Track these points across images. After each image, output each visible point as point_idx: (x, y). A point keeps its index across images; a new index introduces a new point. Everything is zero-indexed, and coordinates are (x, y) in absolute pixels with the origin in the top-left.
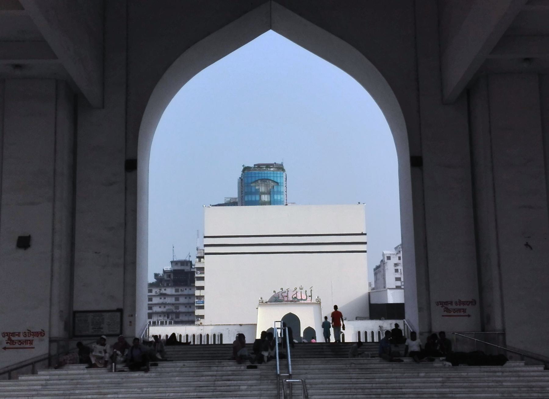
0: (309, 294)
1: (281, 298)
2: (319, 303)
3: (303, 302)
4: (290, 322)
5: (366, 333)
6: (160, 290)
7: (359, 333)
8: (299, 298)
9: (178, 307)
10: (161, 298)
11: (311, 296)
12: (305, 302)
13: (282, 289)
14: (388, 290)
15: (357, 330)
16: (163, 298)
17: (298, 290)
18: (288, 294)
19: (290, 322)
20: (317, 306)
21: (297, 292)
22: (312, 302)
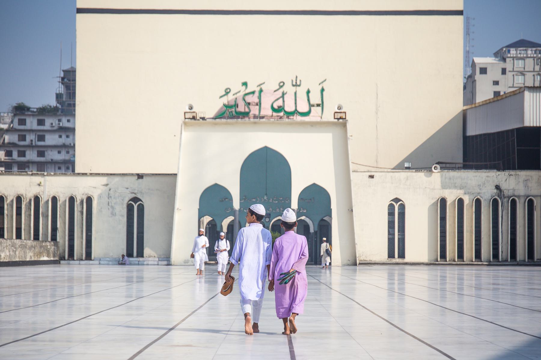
0: (315, 99)
1: (242, 108)
2: (341, 120)
3: (299, 118)
6: (60, 121)
8: (289, 107)
9: (25, 136)
10: (60, 137)
11: (321, 105)
12: (306, 119)
13: (245, 84)
14: (527, 94)
16: (64, 136)
18: (260, 97)
20: (338, 130)
21: (284, 94)
22: (324, 119)
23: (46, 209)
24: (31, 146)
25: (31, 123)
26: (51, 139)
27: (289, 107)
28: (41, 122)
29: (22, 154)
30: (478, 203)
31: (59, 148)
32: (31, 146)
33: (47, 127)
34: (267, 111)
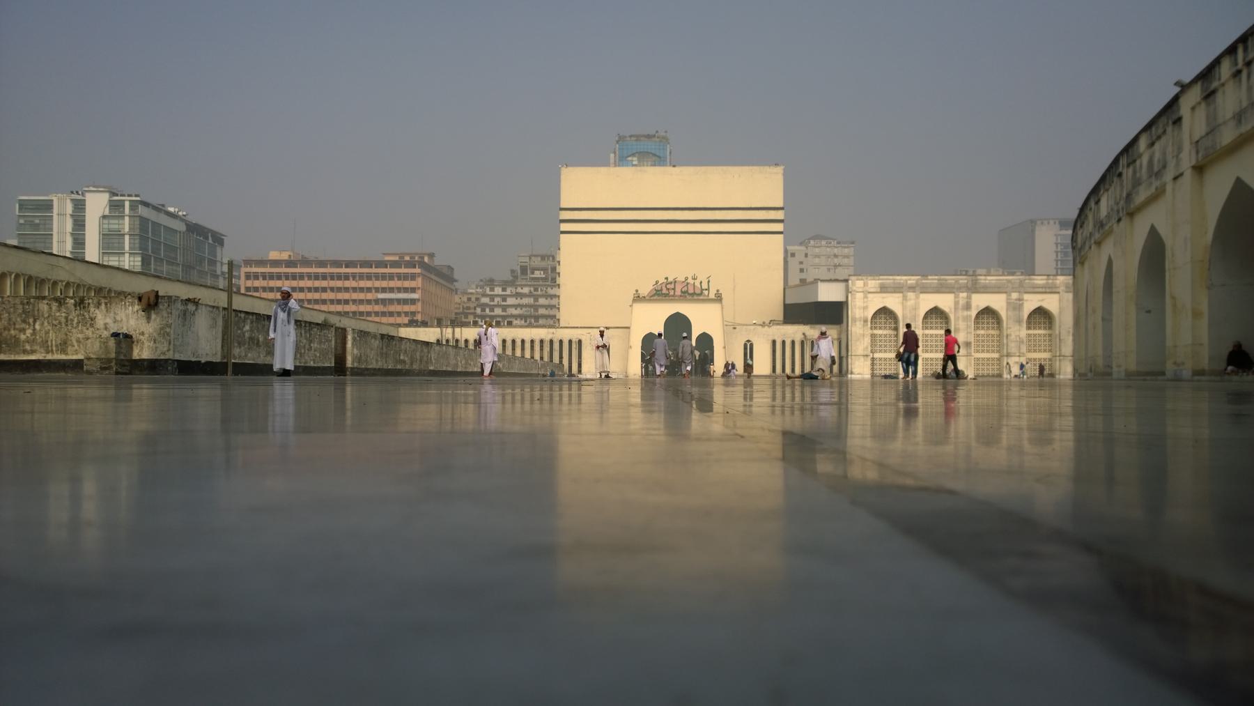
0: (705, 286)
1: (664, 291)
2: (719, 298)
4: (678, 324)
5: (784, 342)
7: (774, 342)
8: (691, 291)
11: (708, 289)
15: (771, 338)
17: (690, 281)
19: (678, 324)
23: (556, 346)
24: (498, 306)
25: (498, 291)
26: (510, 301)
27: (691, 291)
28: (504, 290)
29: (492, 310)
30: (793, 342)
31: (516, 306)
32: (498, 306)
33: (508, 292)
34: (678, 292)
